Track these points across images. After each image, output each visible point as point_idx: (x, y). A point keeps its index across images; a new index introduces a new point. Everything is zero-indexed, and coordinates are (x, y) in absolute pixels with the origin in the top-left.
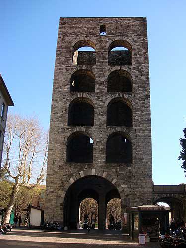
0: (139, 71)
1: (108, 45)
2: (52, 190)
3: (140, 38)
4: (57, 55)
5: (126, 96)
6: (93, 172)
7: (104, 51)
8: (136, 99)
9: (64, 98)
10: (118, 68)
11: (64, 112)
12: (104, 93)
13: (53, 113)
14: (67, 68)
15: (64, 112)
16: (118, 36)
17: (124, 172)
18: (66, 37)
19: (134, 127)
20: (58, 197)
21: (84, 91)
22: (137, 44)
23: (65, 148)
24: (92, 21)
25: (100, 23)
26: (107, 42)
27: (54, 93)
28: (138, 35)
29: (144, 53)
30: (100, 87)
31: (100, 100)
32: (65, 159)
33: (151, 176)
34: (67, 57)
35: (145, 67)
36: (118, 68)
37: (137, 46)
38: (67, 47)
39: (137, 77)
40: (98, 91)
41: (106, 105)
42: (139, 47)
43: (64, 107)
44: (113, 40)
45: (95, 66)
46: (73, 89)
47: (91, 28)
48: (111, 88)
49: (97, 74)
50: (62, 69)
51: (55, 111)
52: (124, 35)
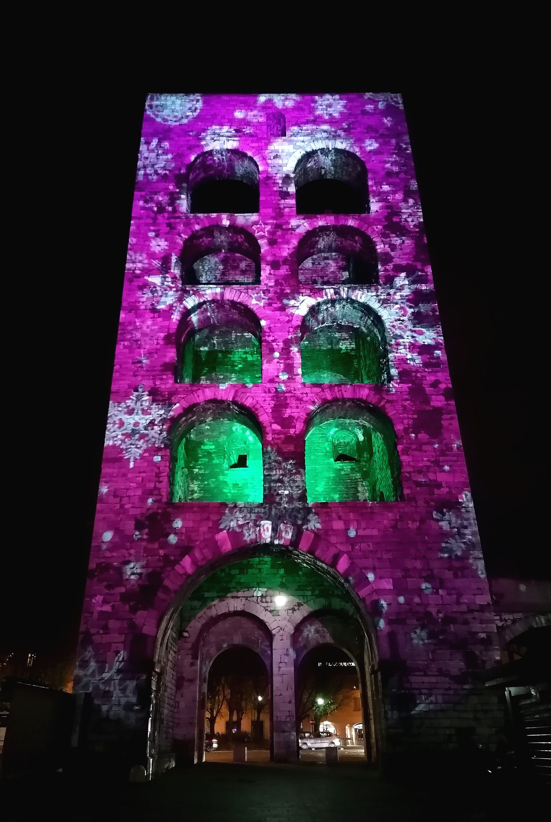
2: (107, 608)
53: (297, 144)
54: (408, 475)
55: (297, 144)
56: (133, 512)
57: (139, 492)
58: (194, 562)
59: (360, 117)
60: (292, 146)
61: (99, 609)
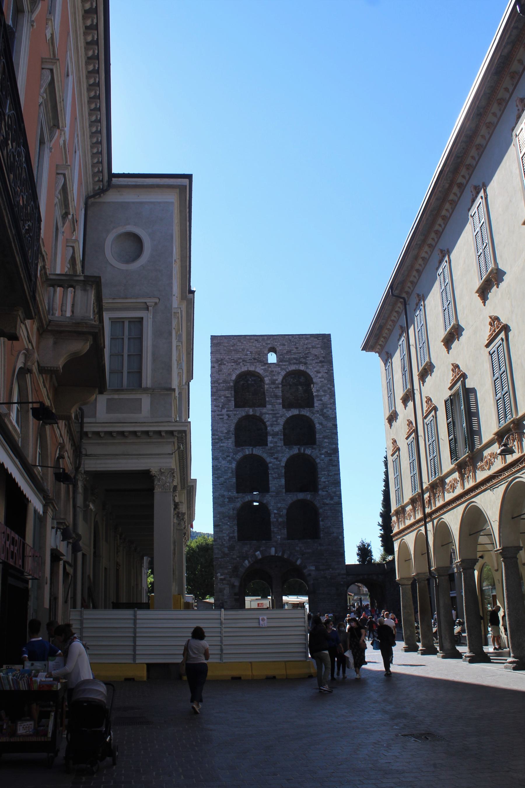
0: (323, 415)
1: (280, 378)
2: (222, 577)
3: (322, 366)
4: (213, 394)
5: (308, 452)
6: (273, 551)
7: (276, 388)
8: (321, 454)
9: (227, 456)
10: (295, 412)
11: (230, 475)
12: (279, 449)
13: (215, 478)
14: (229, 413)
15: (230, 475)
16: (295, 364)
17: (310, 551)
18: (223, 367)
19: (320, 492)
20: (233, 586)
21: (255, 446)
22: (320, 375)
23: (236, 522)
24: (256, 341)
25: (267, 344)
26: (279, 373)
27: (213, 450)
28: (321, 362)
29: (329, 388)
30: (275, 440)
31: (275, 458)
32: (236, 538)
33: (342, 554)
34: (228, 397)
35: (331, 409)
36: (295, 412)
37: (320, 378)
38: (225, 381)
39: (321, 424)
40: (272, 445)
41: (283, 464)
42: (323, 380)
43: (229, 468)
44: (288, 371)
45: (264, 410)
46: (239, 443)
47: (256, 352)
48: (288, 442)
49: (268, 421)
50: (221, 415)
51: (217, 474)
52: (301, 363)
53: (283, 367)
54: (322, 529)
55: (283, 367)
56: (226, 545)
57: (228, 538)
58: (249, 562)
59: (311, 349)
60: (280, 368)
61: (220, 577)
